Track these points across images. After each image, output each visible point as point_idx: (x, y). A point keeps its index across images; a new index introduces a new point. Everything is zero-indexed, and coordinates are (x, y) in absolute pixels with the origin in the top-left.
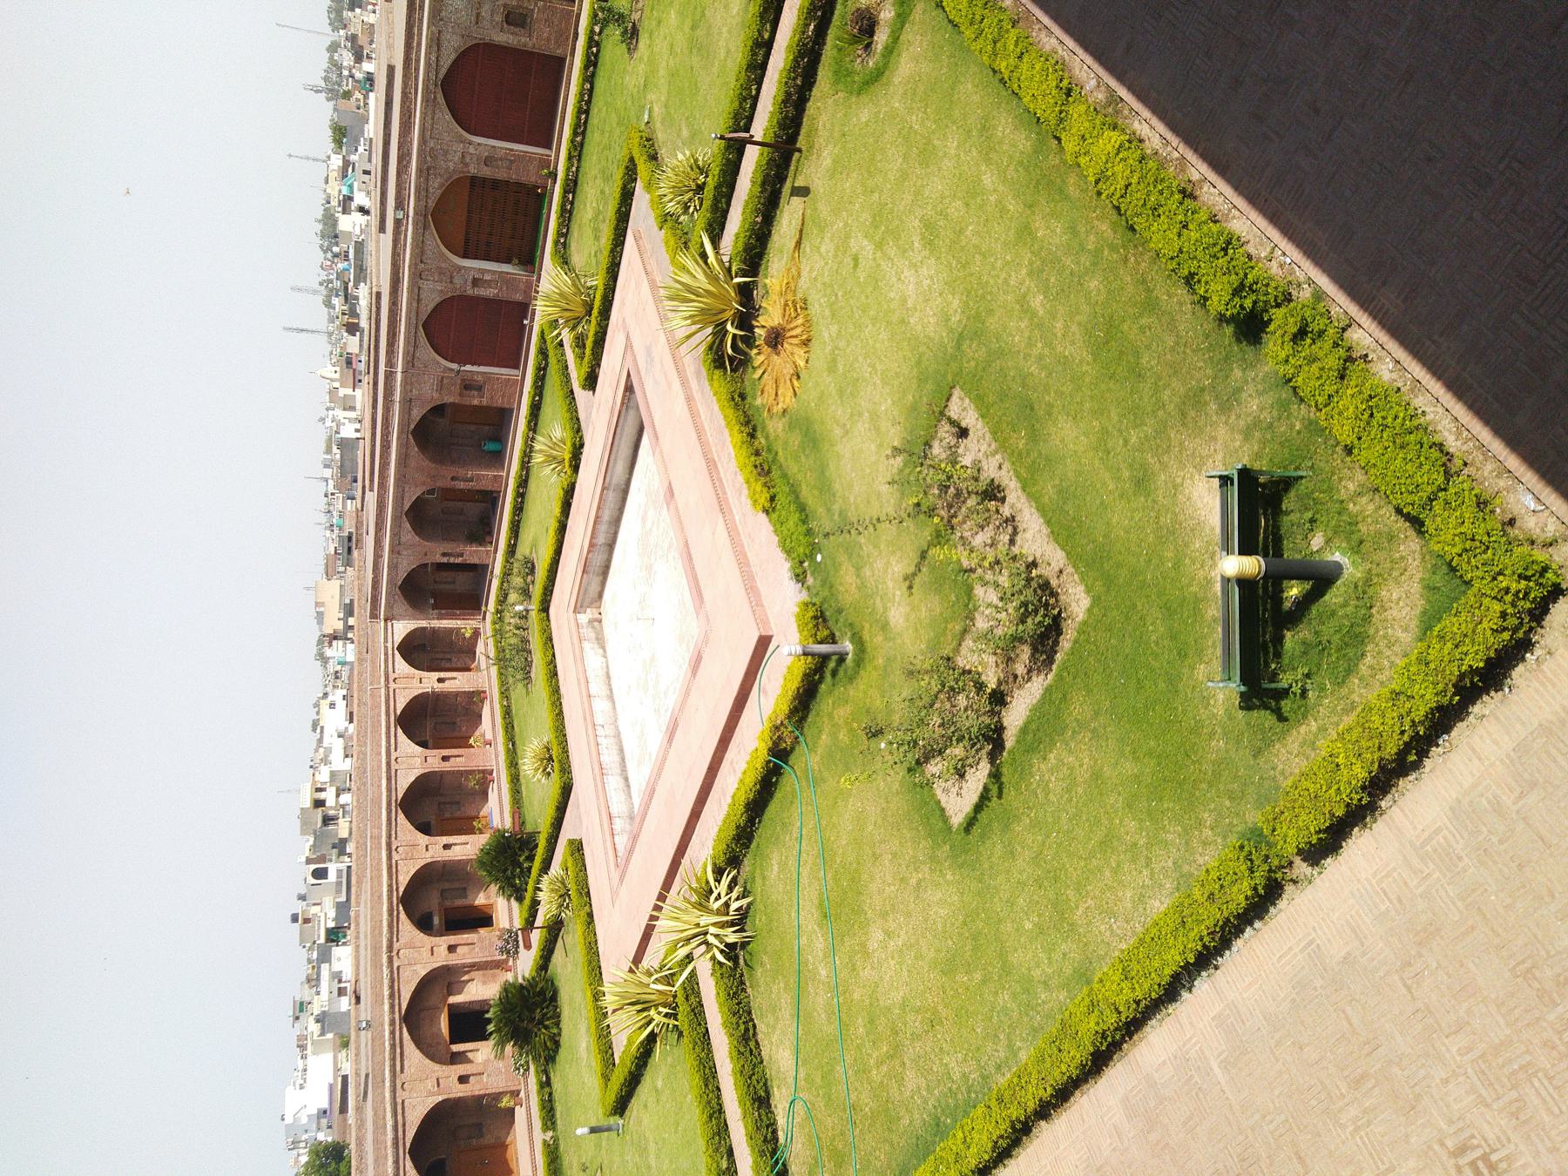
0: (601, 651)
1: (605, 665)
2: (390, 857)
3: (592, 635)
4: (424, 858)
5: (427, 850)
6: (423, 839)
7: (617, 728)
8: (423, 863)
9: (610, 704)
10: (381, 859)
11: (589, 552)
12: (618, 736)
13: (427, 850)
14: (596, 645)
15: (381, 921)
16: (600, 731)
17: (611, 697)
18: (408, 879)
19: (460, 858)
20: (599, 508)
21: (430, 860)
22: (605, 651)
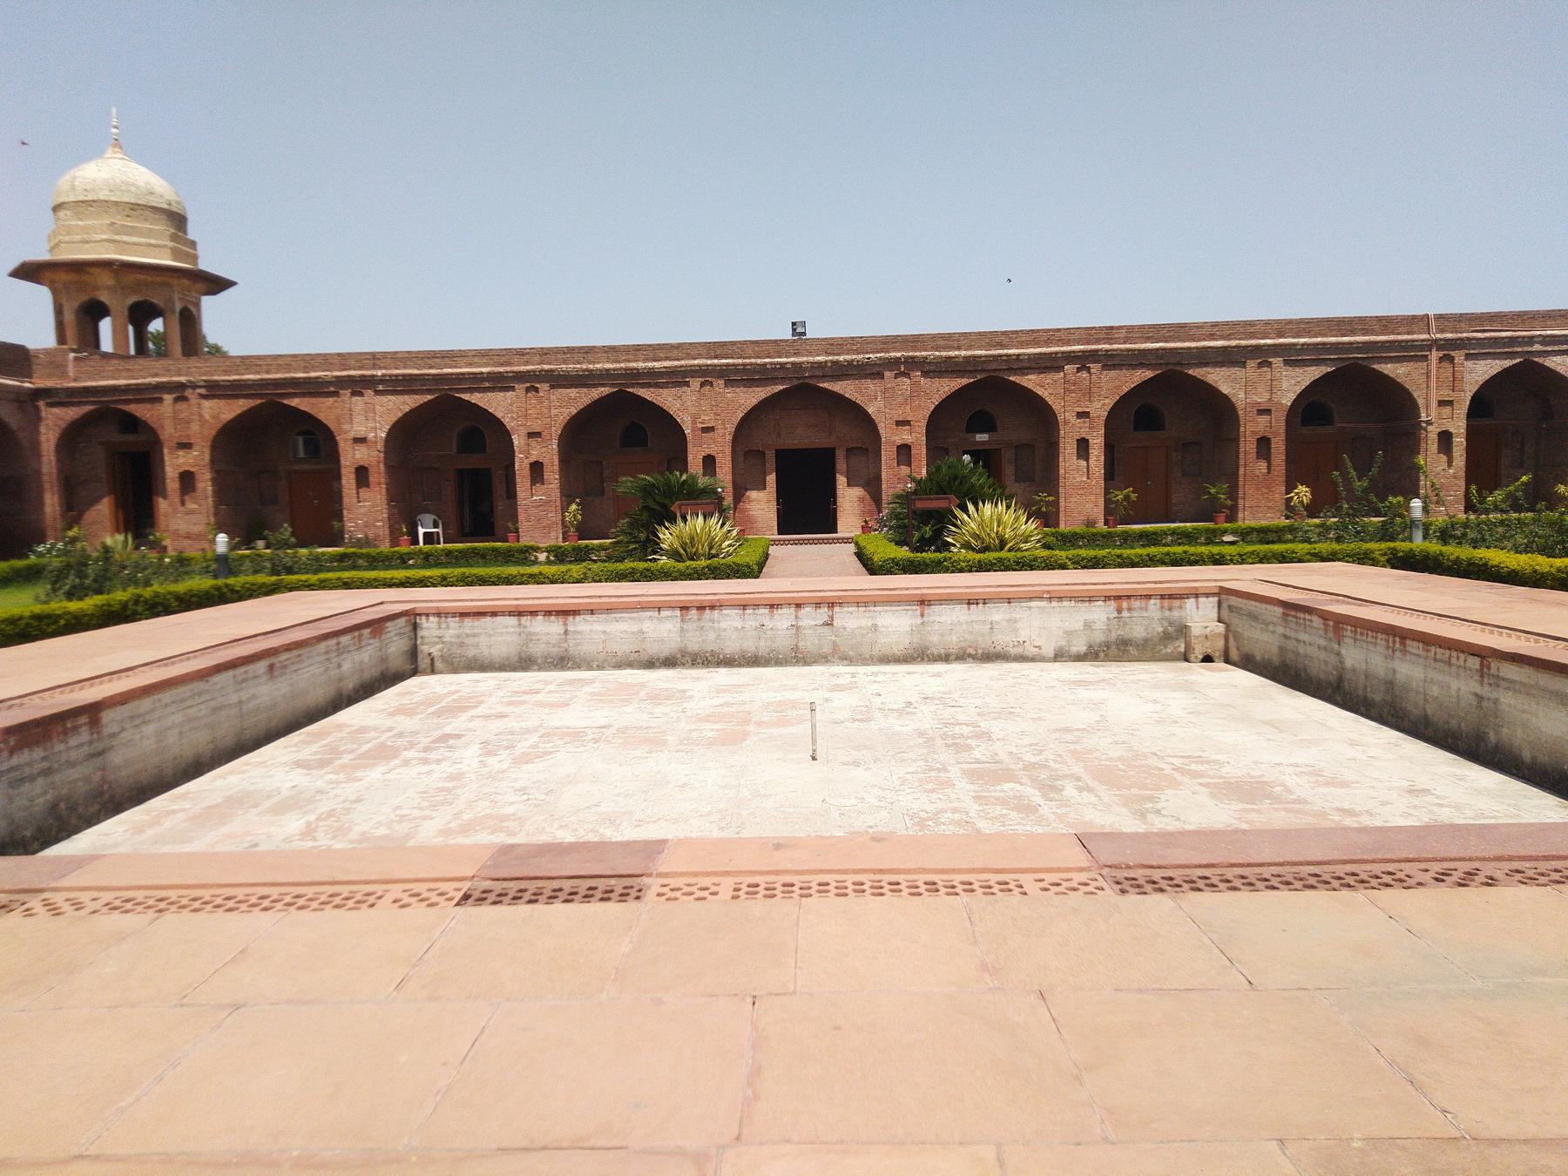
0: (1080, 647)
1: (1031, 651)
2: (1070, 358)
3: (1138, 631)
4: (1065, 412)
5: (1080, 415)
6: (1100, 407)
7: (822, 659)
8: (1056, 406)
9: (897, 650)
10: (1068, 343)
11: (1325, 616)
12: (798, 658)
13: (1080, 415)
14: (1099, 637)
15: (959, 348)
16: (811, 618)
17: (919, 655)
18: (1030, 386)
19: (1062, 464)
20: (1427, 640)
21: (1060, 418)
22: (1080, 658)
